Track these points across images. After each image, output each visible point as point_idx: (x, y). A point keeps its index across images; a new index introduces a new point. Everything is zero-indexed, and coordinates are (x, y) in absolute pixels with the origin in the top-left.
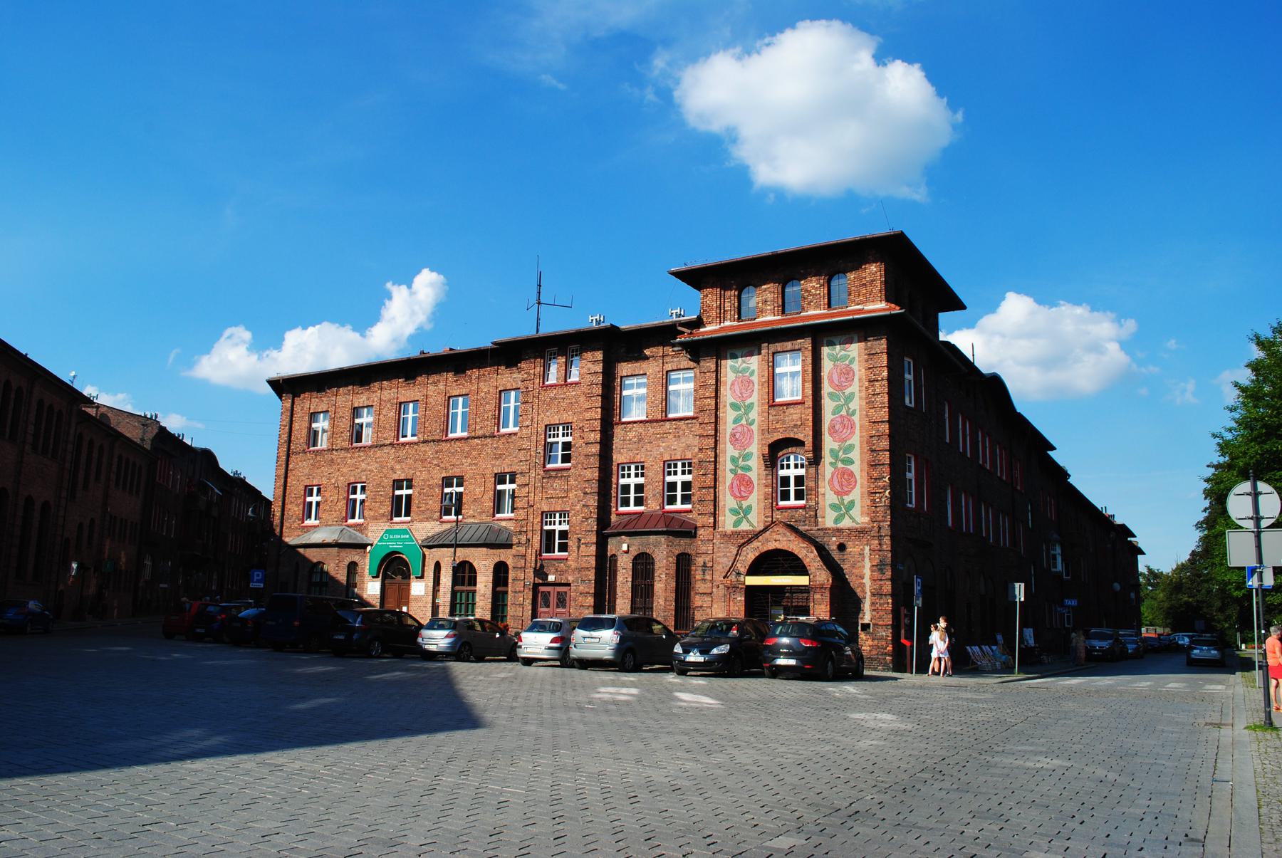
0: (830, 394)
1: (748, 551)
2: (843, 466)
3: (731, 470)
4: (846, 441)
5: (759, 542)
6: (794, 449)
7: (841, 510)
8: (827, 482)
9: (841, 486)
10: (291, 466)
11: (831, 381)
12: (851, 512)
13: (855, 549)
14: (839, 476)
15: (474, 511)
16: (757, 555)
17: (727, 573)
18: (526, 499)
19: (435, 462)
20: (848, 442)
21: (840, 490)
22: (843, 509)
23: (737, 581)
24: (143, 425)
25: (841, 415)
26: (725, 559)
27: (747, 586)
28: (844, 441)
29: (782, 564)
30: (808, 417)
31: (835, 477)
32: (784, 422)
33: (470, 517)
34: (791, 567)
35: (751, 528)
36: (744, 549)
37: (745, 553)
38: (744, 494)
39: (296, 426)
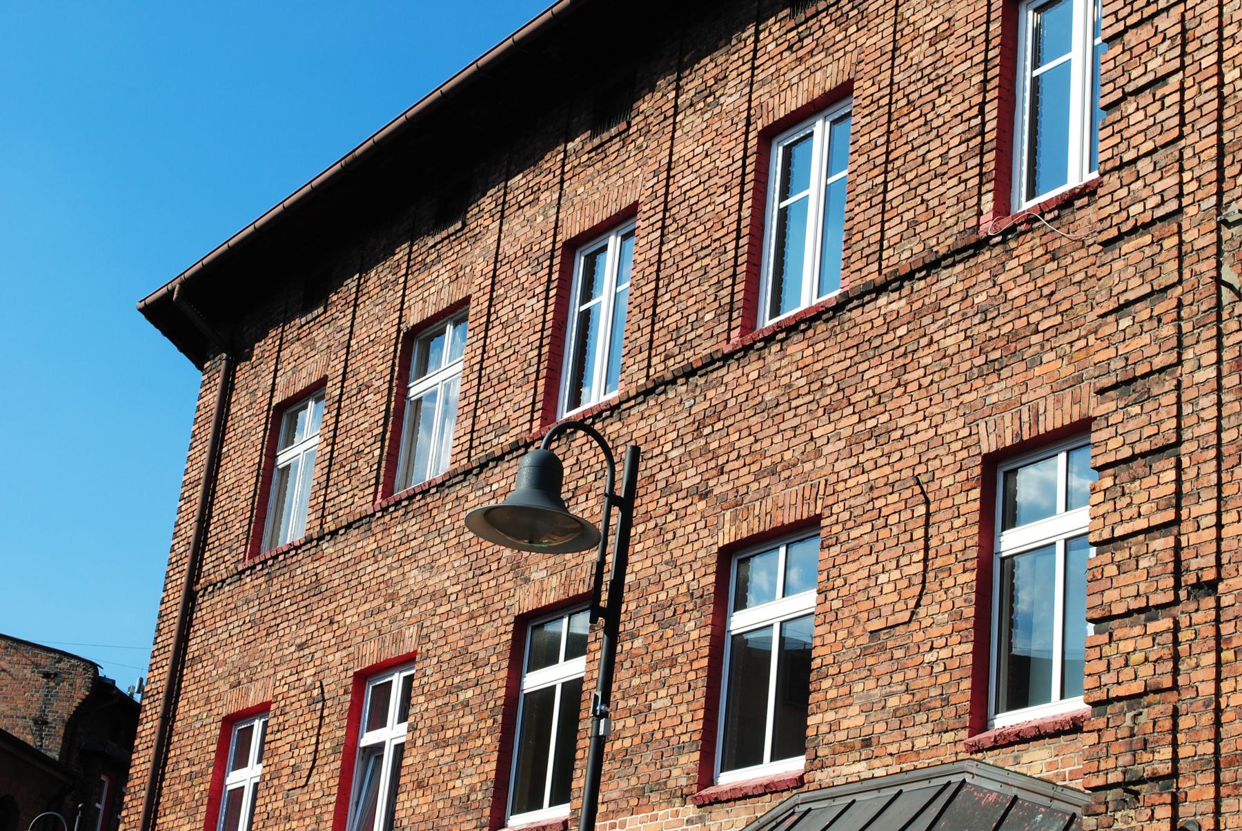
10: (194, 647)
15: (866, 711)
18: (1162, 543)
19: (690, 479)
24: (47, 676)
33: (846, 747)
39: (227, 476)
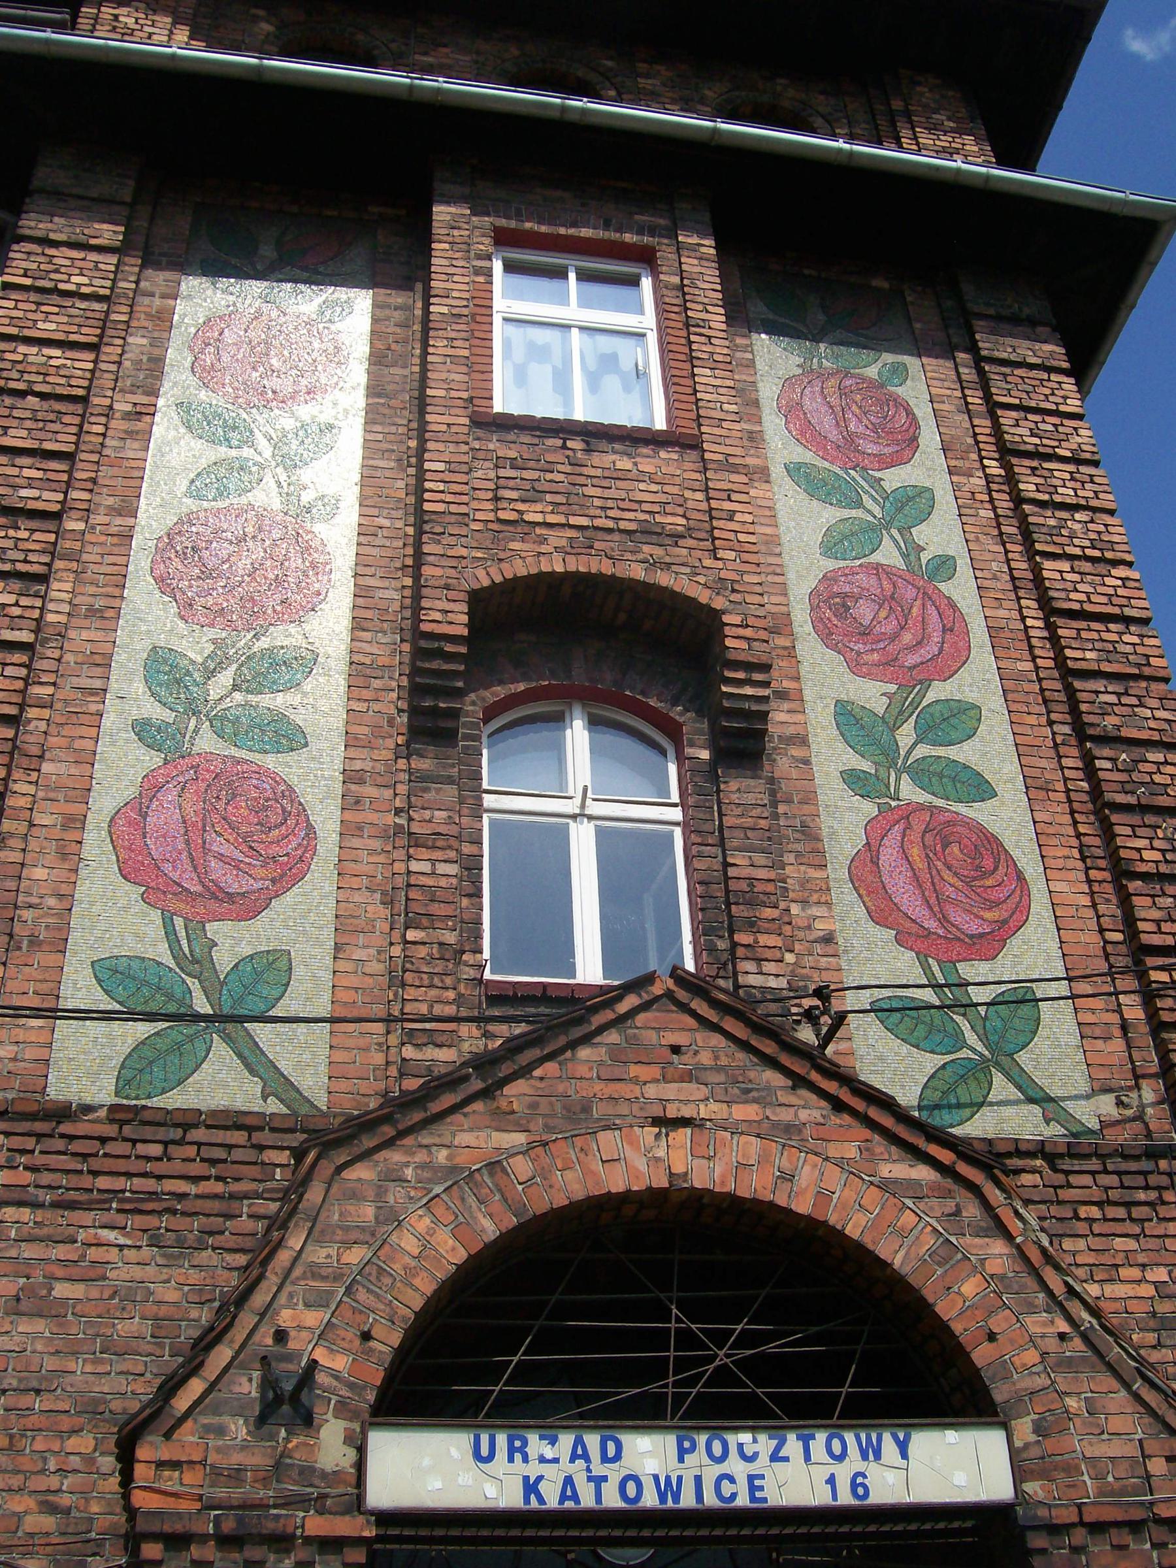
0: (794, 470)
1: (395, 1195)
2: (922, 797)
3: (143, 730)
4: (926, 683)
5: (504, 1120)
6: (607, 679)
7: (959, 1042)
8: (838, 872)
9: (938, 905)
11: (791, 410)
12: (1023, 1057)
13: (1120, 1290)
14: (915, 852)
16: (489, 1229)
17: (171, 1386)
20: (938, 691)
21: (931, 924)
22: (971, 1038)
23: (279, 1468)
25: (878, 566)
26: (40, 1326)
27: (386, 1518)
28: (921, 677)
29: (686, 1339)
30: (727, 505)
31: (889, 855)
32: (571, 501)
34: (758, 1369)
35: (274, 1106)
36: (362, 1172)
37: (368, 1212)
38: (233, 883)
